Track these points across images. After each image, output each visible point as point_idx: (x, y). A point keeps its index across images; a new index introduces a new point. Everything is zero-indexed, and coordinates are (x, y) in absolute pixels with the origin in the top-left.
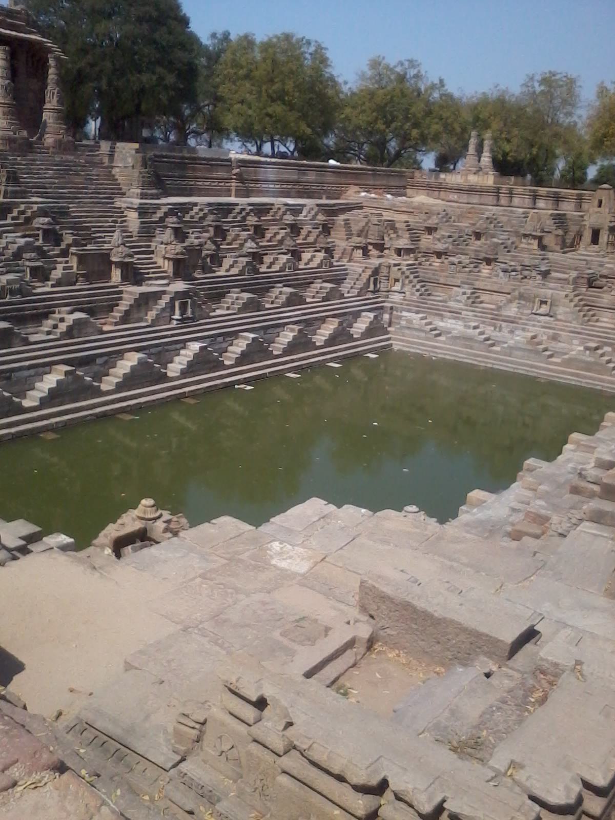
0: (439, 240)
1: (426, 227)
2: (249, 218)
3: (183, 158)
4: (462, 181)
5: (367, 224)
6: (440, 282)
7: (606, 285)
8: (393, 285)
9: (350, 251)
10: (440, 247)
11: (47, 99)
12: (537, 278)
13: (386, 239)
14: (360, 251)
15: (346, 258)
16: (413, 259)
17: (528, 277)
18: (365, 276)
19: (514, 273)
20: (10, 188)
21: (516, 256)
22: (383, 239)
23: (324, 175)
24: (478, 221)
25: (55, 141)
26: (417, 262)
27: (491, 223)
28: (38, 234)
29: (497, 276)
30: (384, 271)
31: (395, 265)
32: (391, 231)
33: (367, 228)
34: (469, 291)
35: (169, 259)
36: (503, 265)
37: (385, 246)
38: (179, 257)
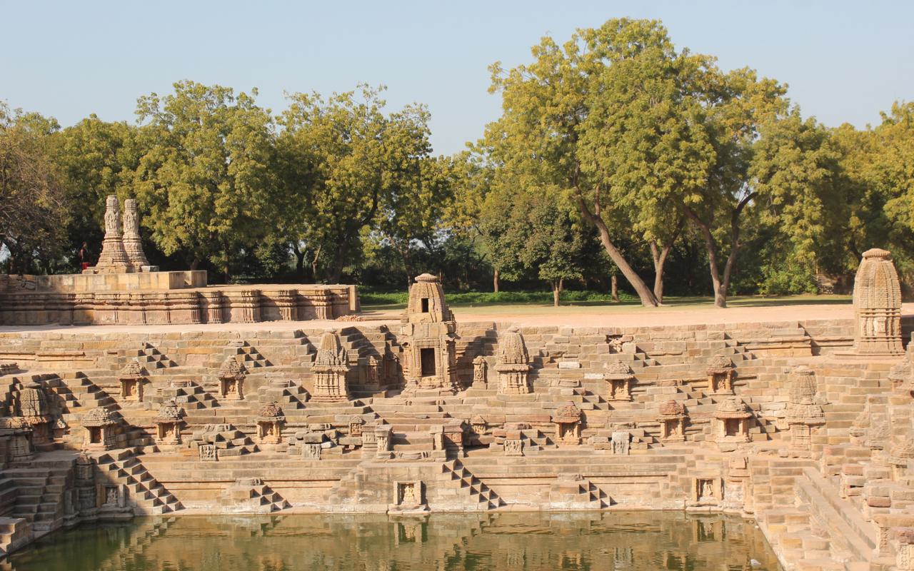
0: (160, 401)
1: (122, 380)
4: (109, 287)
5: (13, 388)
6: (191, 480)
7: (492, 441)
10: (165, 414)
12: (379, 445)
16: (124, 444)
17: (352, 447)
19: (328, 444)
21: (316, 412)
24: (222, 359)
26: (132, 449)
27: (248, 358)
29: (298, 452)
34: (259, 489)
36: (301, 432)
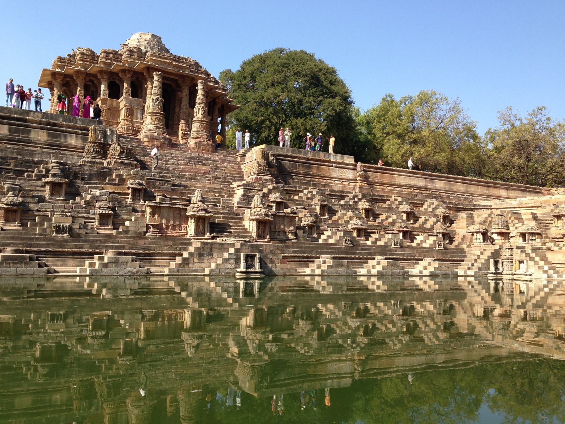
2: (360, 203)
3: (308, 159)
5: (490, 215)
8: (517, 268)
9: (470, 237)
11: (195, 114)
13: (511, 228)
14: (480, 236)
15: (466, 243)
18: (484, 257)
22: (508, 229)
23: (453, 185)
25: (196, 143)
28: (128, 194)
30: (507, 253)
31: (518, 247)
32: (516, 221)
33: (490, 219)
35: (252, 220)
37: (510, 235)
38: (262, 218)
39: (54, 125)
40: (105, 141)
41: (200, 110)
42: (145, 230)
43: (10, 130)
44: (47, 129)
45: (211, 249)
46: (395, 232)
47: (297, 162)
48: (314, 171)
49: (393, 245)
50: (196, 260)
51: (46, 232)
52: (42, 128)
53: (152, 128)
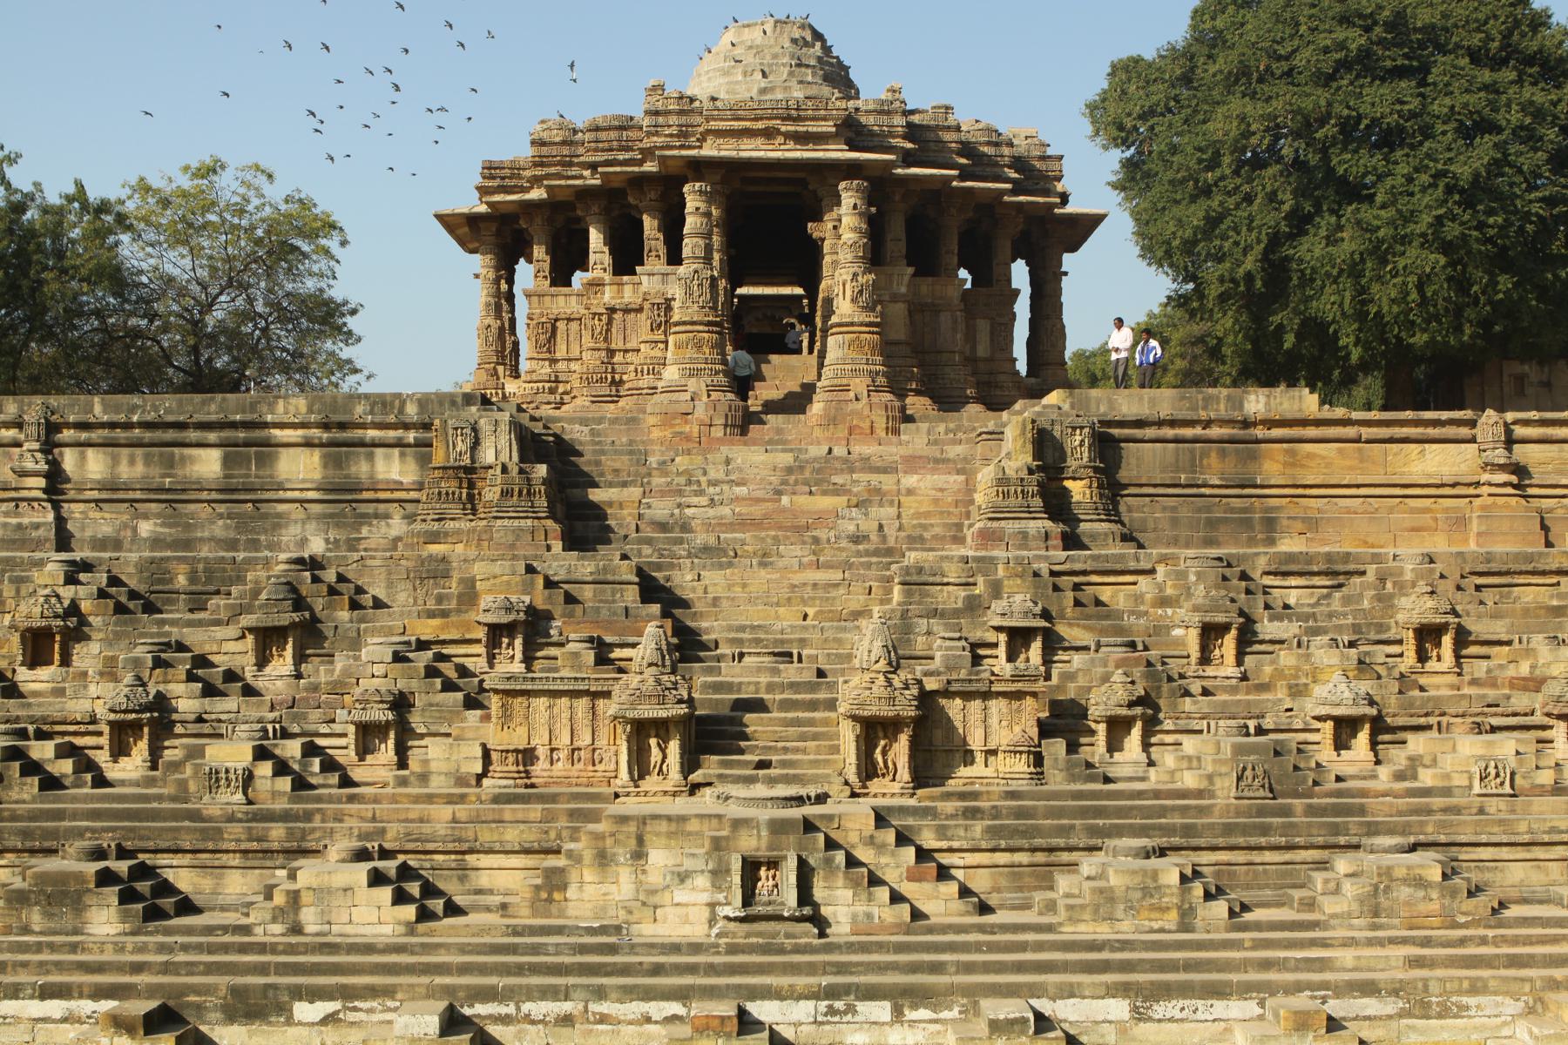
2: (1403, 602)
20: (499, 522)
39: (342, 426)
40: (473, 461)
41: (848, 286)
42: (480, 771)
43: (227, 462)
44: (321, 445)
45: (640, 840)
46: (1538, 719)
47: (1195, 440)
48: (1272, 467)
49: (1476, 782)
50: (589, 875)
51: (186, 790)
52: (308, 444)
53: (677, 377)
